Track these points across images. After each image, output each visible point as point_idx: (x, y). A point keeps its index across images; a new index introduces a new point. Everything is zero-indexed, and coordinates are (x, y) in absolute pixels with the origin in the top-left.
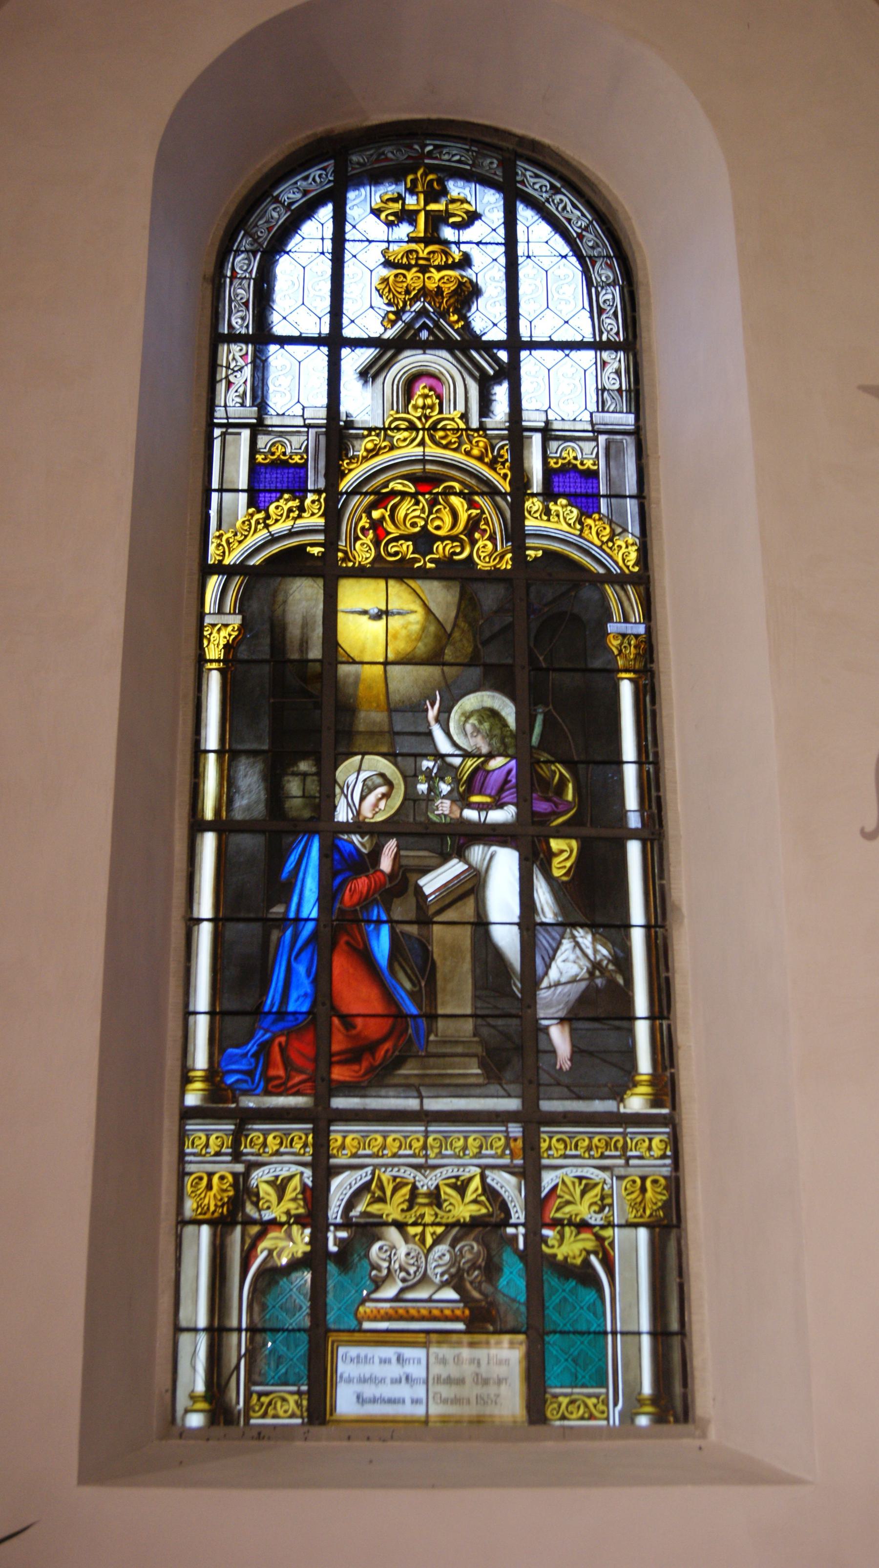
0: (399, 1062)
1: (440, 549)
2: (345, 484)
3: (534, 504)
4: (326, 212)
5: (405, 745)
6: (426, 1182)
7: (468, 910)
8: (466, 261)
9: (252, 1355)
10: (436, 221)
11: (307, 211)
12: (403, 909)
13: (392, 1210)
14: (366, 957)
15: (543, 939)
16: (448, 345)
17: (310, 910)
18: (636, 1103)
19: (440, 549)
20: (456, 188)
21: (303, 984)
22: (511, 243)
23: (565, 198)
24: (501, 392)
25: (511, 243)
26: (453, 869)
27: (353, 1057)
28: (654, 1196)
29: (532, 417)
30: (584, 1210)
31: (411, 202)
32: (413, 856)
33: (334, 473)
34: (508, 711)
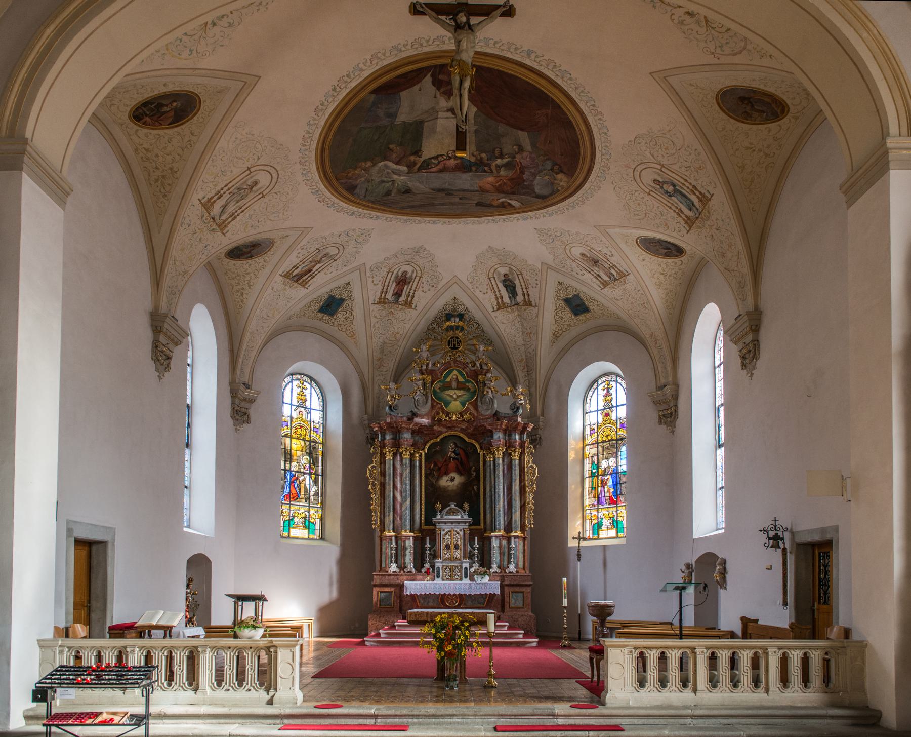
0: (297, 499)
1: (302, 436)
2: (292, 426)
3: (312, 432)
4: (290, 384)
5: (298, 461)
6: (300, 512)
7: (304, 482)
8: (305, 396)
9: (283, 529)
10: (303, 388)
11: (287, 384)
12: (298, 481)
13: (296, 515)
14: (294, 487)
15: (311, 486)
16: (304, 407)
17: (289, 481)
18: (319, 506)
19: (302, 436)
20: (305, 384)
21: (288, 489)
22: (311, 393)
23: (317, 388)
24: (309, 415)
25: (311, 393)
26: (303, 477)
27: (293, 498)
28: (320, 516)
29: (312, 420)
30: (313, 517)
31: (300, 385)
32: (299, 475)
33: (291, 424)
34: (309, 459)
